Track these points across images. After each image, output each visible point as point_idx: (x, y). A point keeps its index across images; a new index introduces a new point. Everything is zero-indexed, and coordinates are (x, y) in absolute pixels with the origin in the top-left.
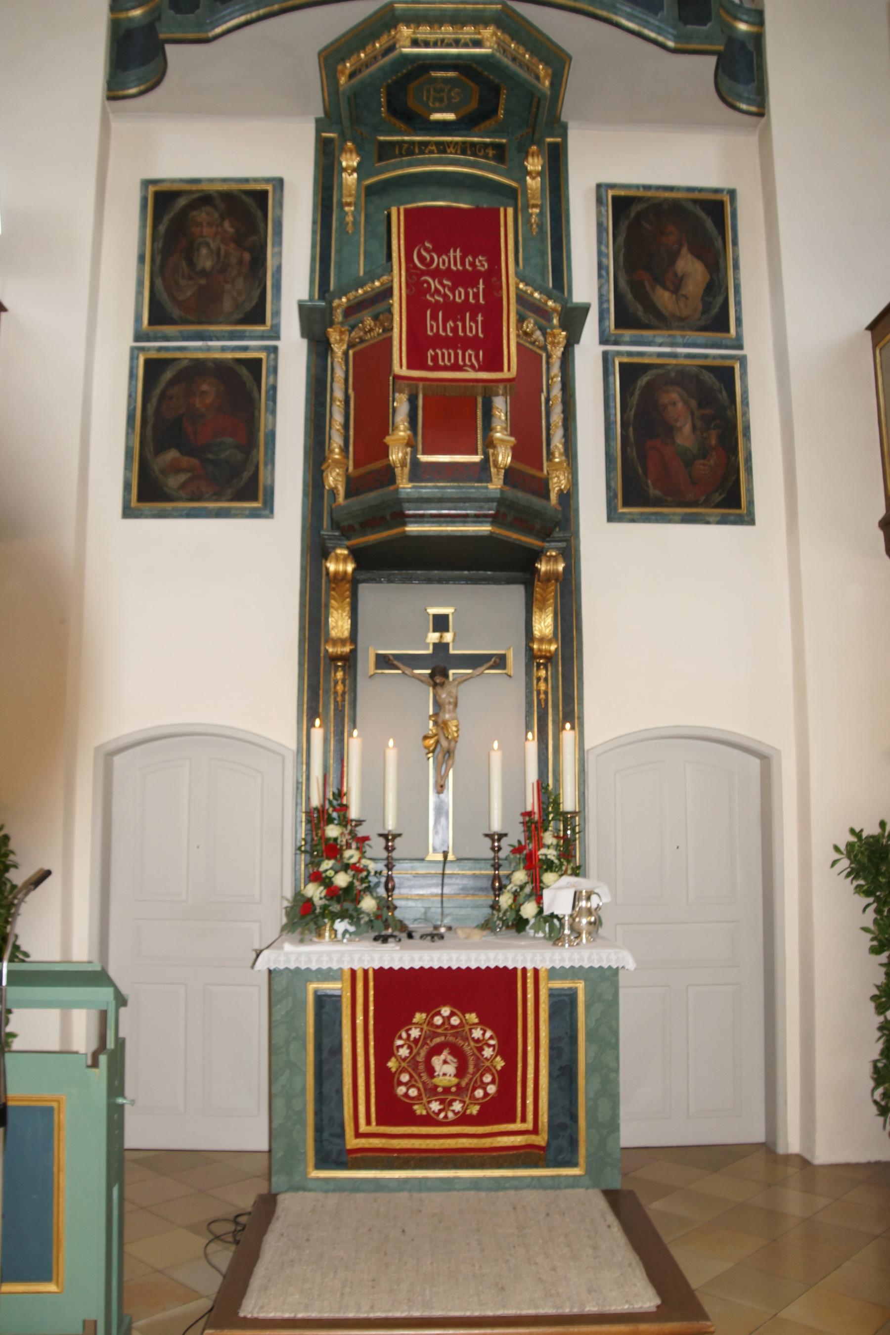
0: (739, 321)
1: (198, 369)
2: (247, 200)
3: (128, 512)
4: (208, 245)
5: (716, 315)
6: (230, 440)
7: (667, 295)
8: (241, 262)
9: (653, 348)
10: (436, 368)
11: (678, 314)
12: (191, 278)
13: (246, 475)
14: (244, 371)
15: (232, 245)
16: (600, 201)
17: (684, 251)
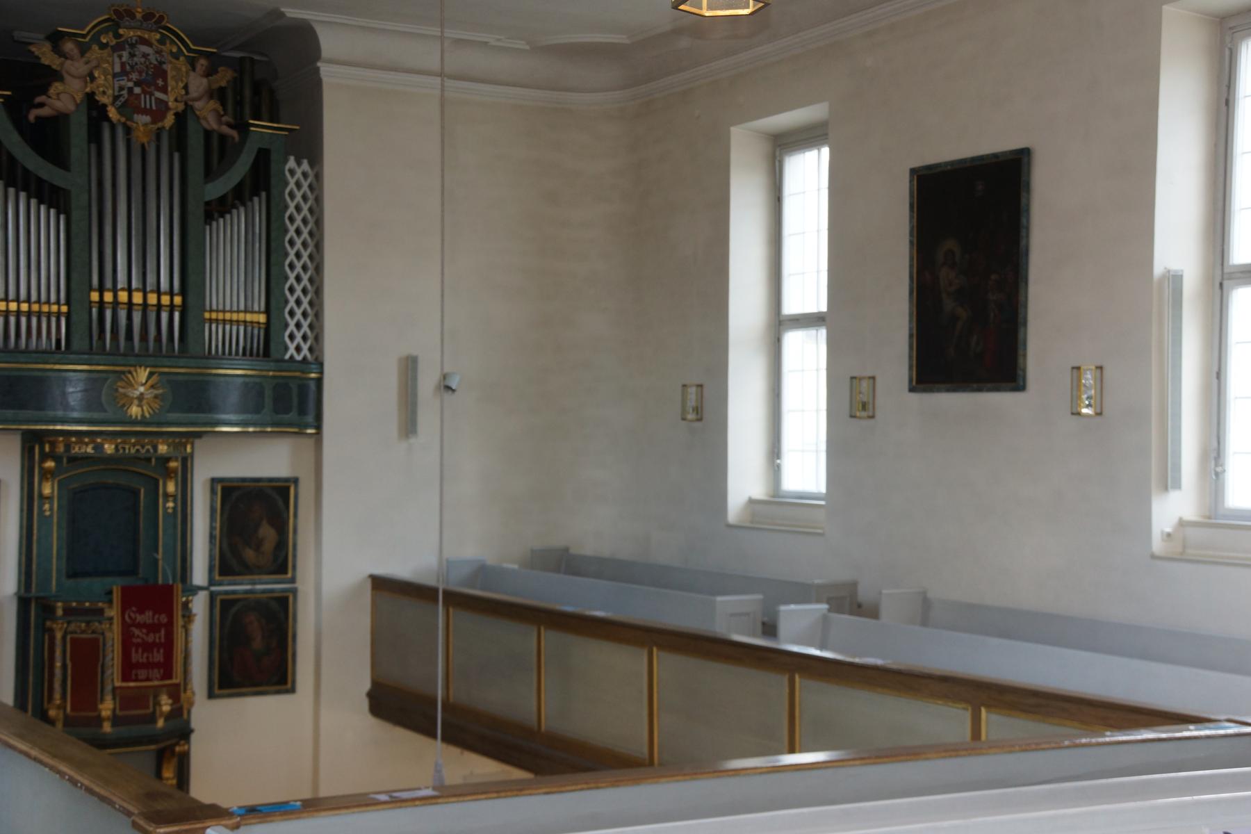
0: (294, 567)
5: (281, 563)
9: (240, 587)
10: (136, 680)
16: (213, 491)
17: (264, 522)
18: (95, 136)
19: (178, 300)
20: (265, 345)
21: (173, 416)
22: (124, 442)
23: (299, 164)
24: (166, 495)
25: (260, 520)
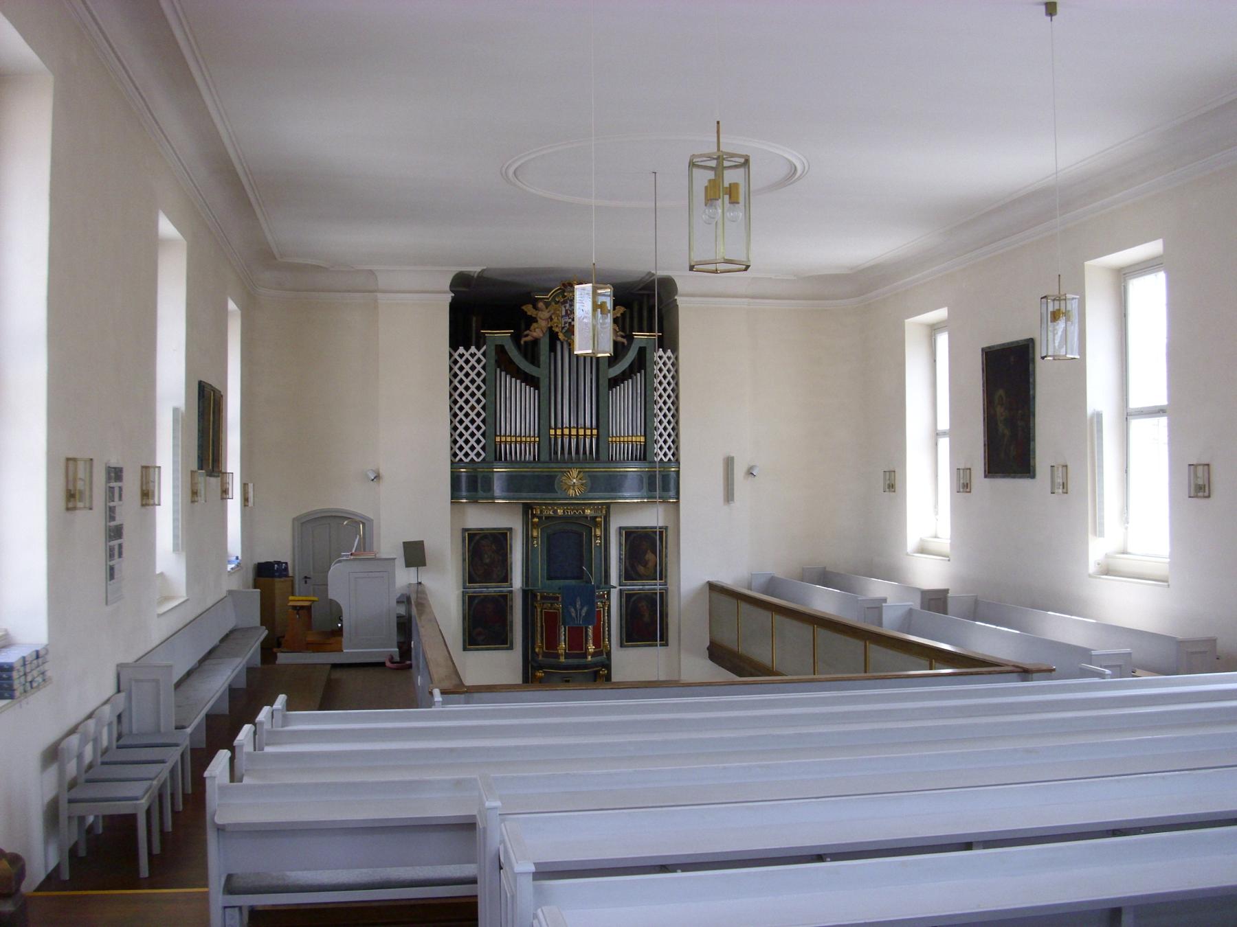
1: (486, 599)
3: (465, 649)
9: (636, 586)
16: (620, 534)
18: (553, 349)
19: (595, 432)
20: (643, 455)
21: (591, 495)
23: (665, 352)
25: (646, 550)
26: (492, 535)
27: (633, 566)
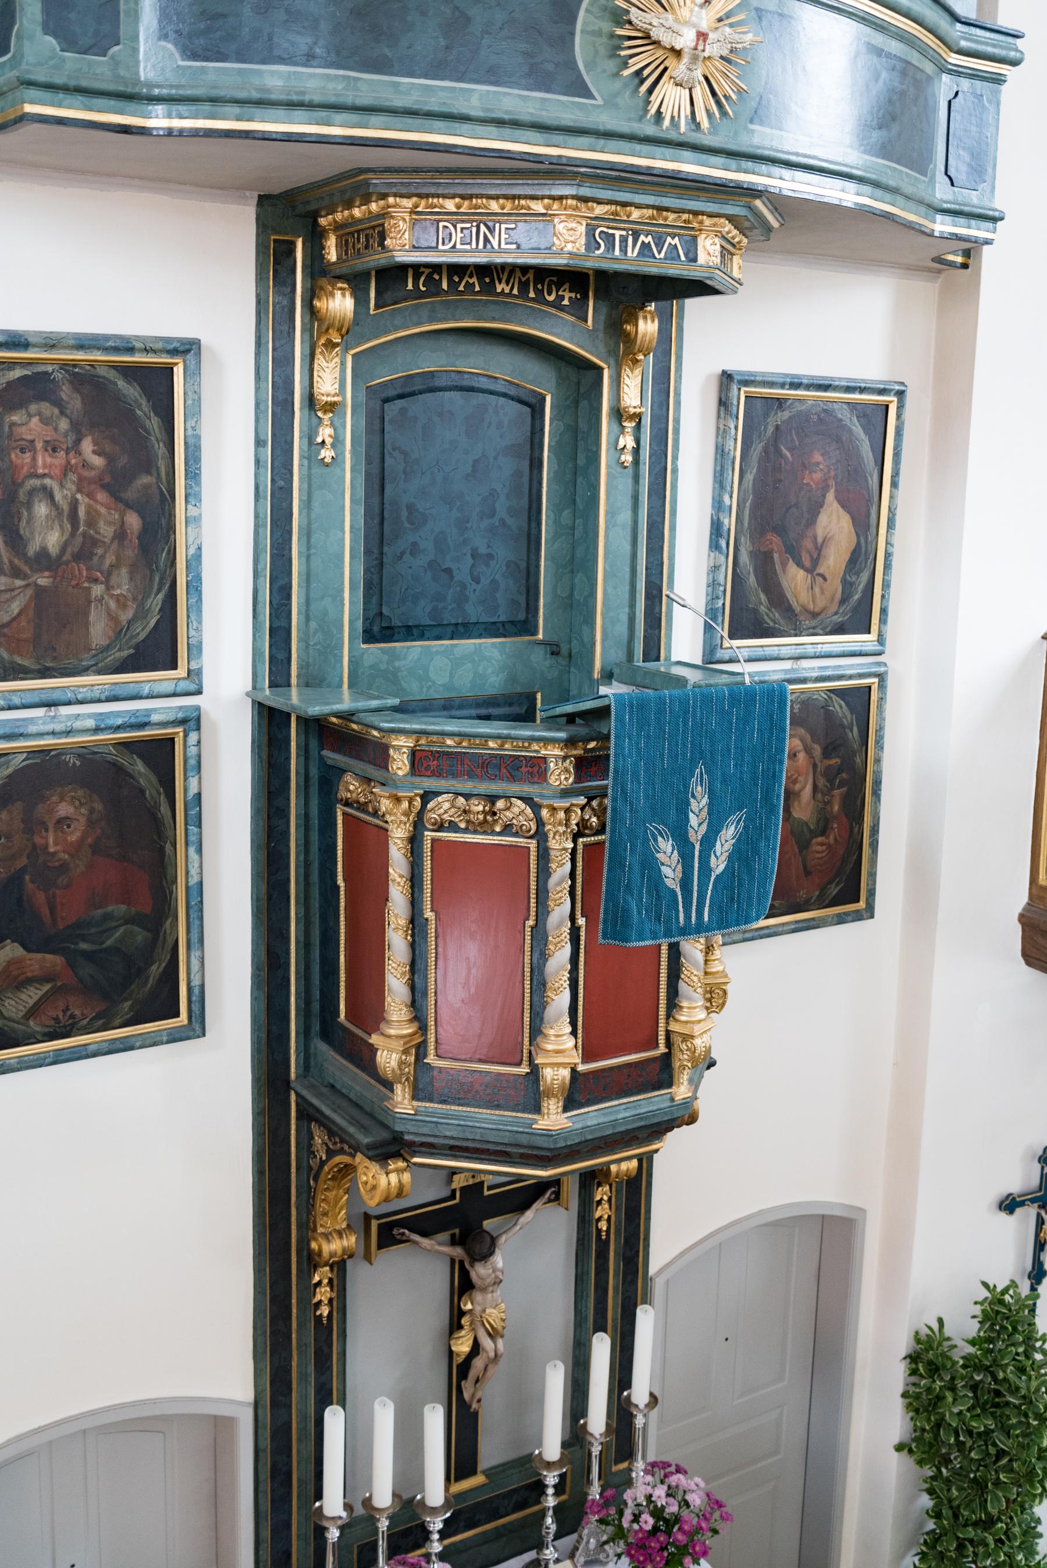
2: (130, 391)
4: (51, 497)
6: (120, 909)
7: (801, 574)
8: (121, 535)
11: (811, 607)
12: (16, 573)
13: (155, 970)
14: (140, 767)
15: (102, 496)
17: (830, 496)
22: (614, 220)
24: (619, 414)
26: (83, 378)
27: (764, 563)
